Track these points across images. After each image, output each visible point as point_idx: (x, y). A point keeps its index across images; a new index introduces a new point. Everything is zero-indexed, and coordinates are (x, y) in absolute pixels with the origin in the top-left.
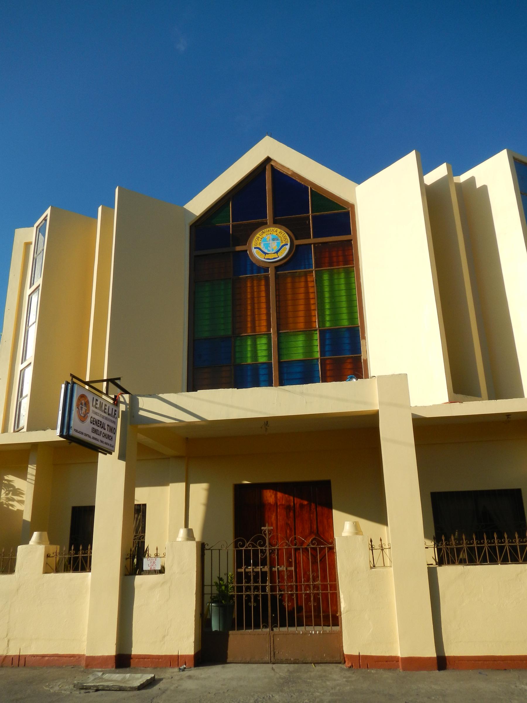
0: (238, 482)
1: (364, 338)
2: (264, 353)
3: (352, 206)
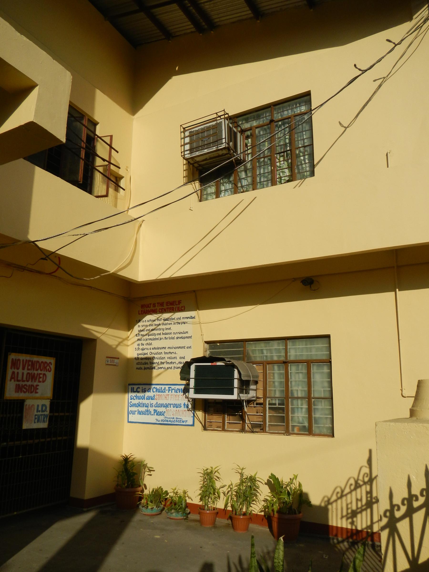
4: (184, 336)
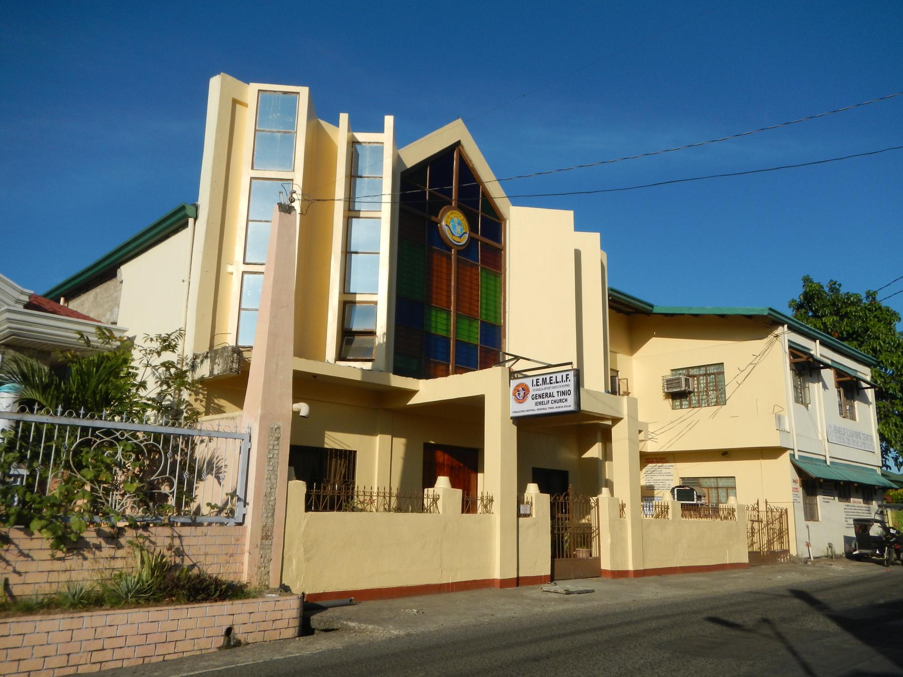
0: (426, 441)
1: (505, 337)
2: (444, 328)
3: (505, 220)
4: (669, 474)
